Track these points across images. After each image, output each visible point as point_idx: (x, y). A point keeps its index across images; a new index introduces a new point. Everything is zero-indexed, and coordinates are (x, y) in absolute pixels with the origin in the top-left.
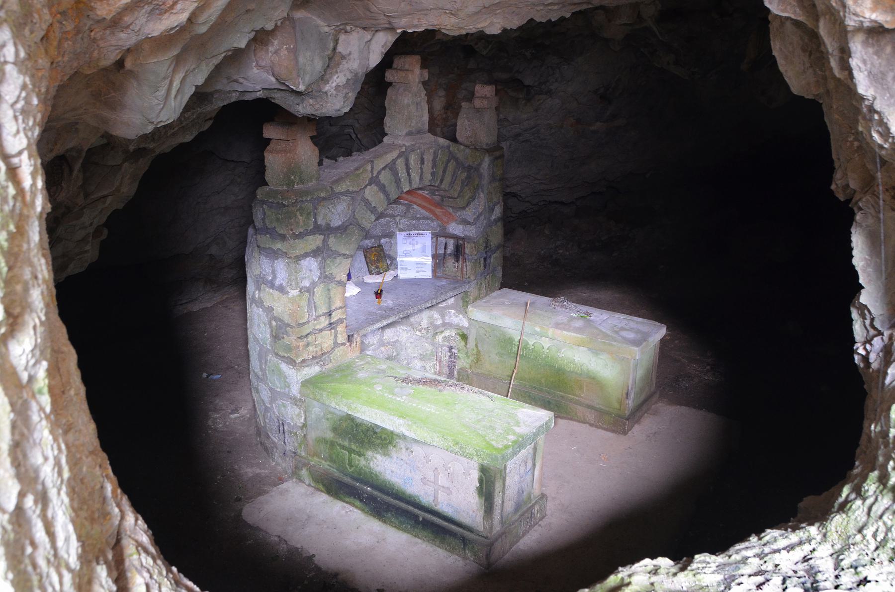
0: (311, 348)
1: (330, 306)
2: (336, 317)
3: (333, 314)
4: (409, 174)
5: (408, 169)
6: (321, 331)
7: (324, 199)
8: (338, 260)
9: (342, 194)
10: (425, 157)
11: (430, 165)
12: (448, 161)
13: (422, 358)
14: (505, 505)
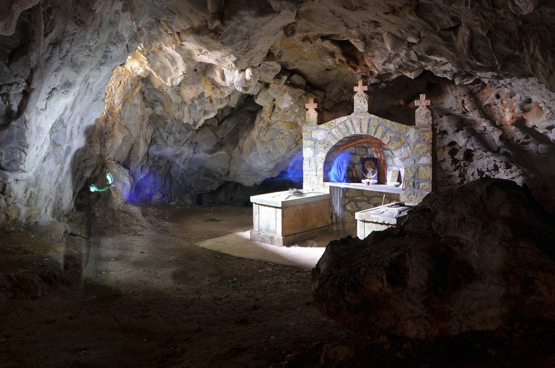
9: (322, 129)
10: (363, 122)
11: (366, 126)
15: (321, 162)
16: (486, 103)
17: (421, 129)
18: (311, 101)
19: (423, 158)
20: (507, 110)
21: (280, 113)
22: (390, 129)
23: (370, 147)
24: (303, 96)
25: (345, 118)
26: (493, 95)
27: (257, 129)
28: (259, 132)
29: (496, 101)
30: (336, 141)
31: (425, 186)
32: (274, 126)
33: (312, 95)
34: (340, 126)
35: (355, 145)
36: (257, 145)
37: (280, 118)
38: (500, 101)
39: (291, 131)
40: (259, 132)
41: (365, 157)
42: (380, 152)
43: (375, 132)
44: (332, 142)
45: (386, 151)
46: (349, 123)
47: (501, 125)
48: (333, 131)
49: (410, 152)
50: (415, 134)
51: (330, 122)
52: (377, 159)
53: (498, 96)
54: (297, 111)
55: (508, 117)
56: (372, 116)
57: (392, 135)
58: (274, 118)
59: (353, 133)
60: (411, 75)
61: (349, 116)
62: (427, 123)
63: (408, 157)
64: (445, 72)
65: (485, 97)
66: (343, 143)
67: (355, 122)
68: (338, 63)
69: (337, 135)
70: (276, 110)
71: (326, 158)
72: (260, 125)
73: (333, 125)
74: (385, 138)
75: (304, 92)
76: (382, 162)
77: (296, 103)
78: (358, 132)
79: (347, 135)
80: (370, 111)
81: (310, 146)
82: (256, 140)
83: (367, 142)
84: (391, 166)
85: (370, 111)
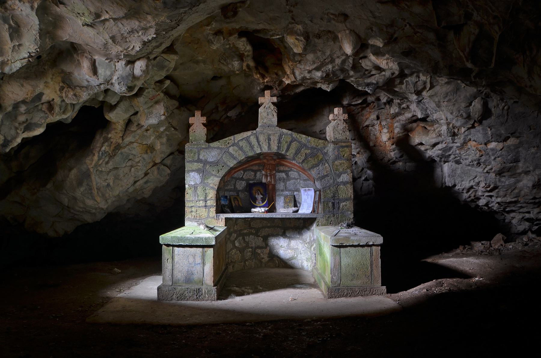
0: (194, 214)
1: (206, 198)
2: (209, 203)
3: (208, 202)
4: (259, 144)
5: (258, 142)
6: (199, 207)
7: (204, 148)
8: (212, 178)
9: (215, 148)
10: (272, 137)
11: (276, 142)
12: (291, 142)
13: (307, 260)
14: (175, 272)
15: (212, 188)
16: (367, 123)
17: (340, 144)
18: (198, 114)
19: (343, 175)
20: (385, 130)
21: (139, 131)
22: (305, 145)
23: (260, 170)
24: (176, 111)
25: (249, 133)
26: (373, 116)
27: (97, 155)
28: (99, 160)
29: (375, 122)
31: (346, 205)
32: (126, 150)
33: (185, 109)
34: (241, 144)
35: (246, 167)
36: (93, 177)
37: (137, 138)
38: (379, 122)
39: (145, 156)
40: (99, 160)
41: (251, 182)
42: (271, 176)
44: (229, 163)
45: (280, 174)
46: (253, 140)
47: (375, 146)
48: (231, 150)
49: (328, 169)
50: (334, 150)
51: (227, 139)
52: (265, 183)
53: (378, 118)
54: (162, 129)
56: (284, 131)
57: (308, 151)
58: (128, 139)
59: (259, 151)
60: (327, 88)
61: (255, 132)
62: (344, 138)
63: (327, 176)
64: (368, 85)
65: (364, 118)
66: (238, 165)
67: (261, 138)
68: (244, 67)
69: (236, 155)
70: (133, 128)
71: (220, 183)
72: (103, 148)
73: (231, 142)
74: (299, 156)
75: (176, 103)
76: (270, 187)
77: (166, 119)
78: (265, 149)
79: (251, 154)
81: (198, 171)
82: (92, 170)
83: (258, 165)
84: (282, 191)
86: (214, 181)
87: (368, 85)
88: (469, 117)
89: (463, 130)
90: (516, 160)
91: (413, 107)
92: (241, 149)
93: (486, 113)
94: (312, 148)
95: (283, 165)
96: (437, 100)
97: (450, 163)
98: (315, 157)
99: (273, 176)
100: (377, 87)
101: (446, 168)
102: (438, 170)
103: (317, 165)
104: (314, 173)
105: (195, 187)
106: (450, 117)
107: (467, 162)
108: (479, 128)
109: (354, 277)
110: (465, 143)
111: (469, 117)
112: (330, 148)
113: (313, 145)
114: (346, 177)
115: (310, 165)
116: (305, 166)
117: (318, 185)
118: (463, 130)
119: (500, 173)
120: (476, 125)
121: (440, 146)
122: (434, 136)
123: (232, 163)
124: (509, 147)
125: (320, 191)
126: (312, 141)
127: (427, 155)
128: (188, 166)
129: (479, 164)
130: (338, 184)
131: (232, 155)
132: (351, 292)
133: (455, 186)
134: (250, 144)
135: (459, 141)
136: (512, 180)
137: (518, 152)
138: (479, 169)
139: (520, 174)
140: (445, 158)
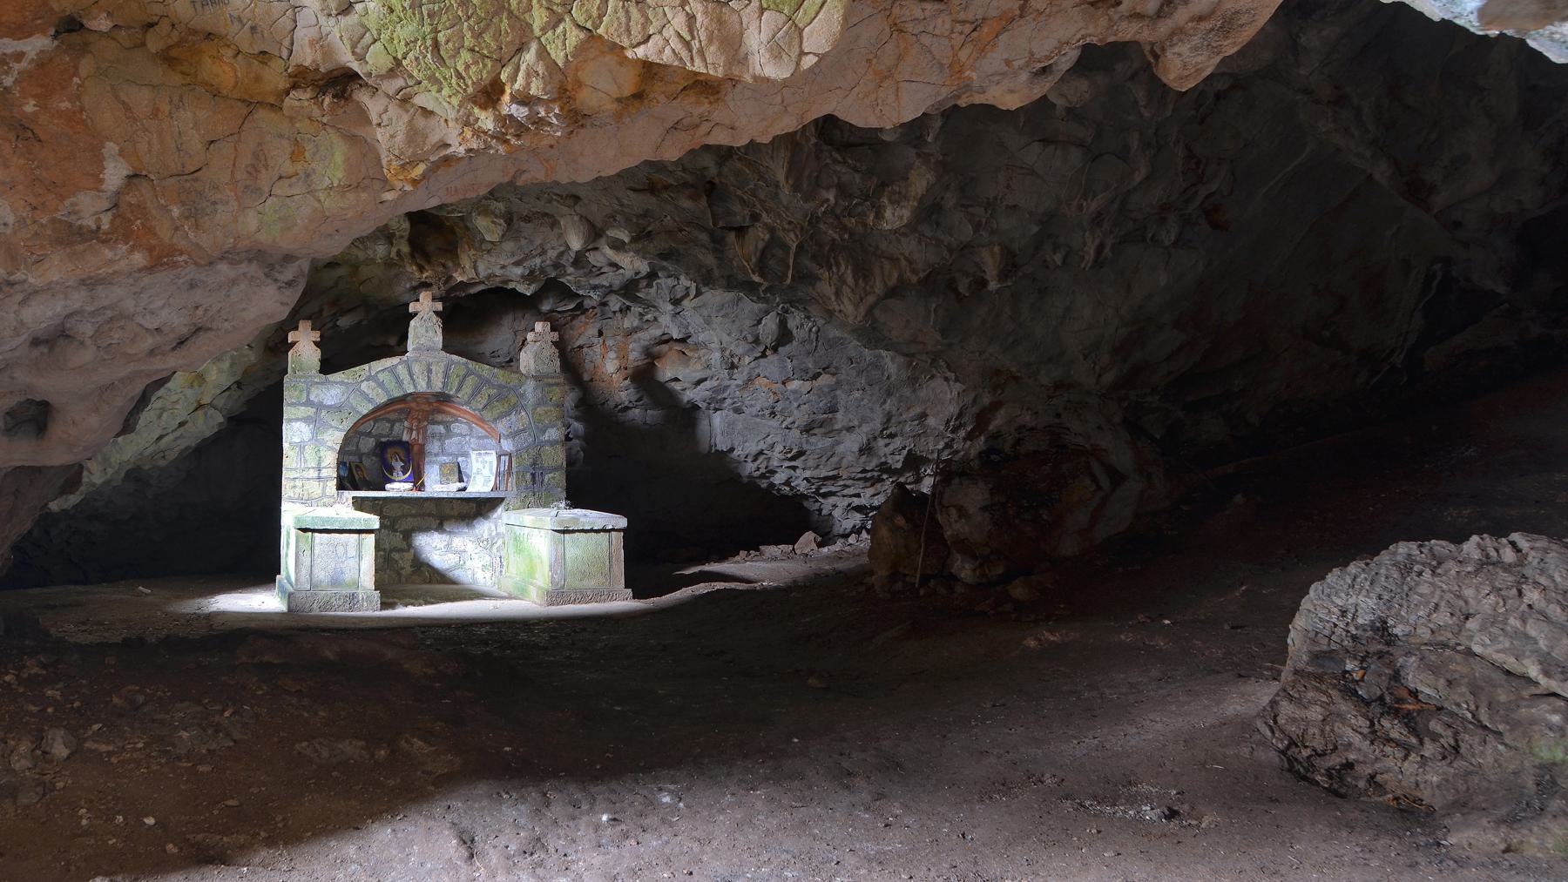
5: (411, 375)
11: (440, 376)
15: (331, 448)
22: (488, 382)
25: (395, 360)
30: (371, 407)
34: (381, 377)
43: (458, 390)
48: (364, 386)
55: (610, 366)
56: (455, 357)
57: (493, 392)
59: (411, 390)
63: (523, 431)
67: (416, 368)
73: (365, 374)
78: (422, 386)
80: (447, 348)
81: (307, 420)
85: (447, 348)
86: (334, 438)
87: (595, 288)
88: (757, 341)
89: (747, 359)
90: (833, 410)
91: (665, 320)
92: (381, 385)
93: (784, 336)
94: (500, 386)
95: (444, 412)
96: (705, 313)
97: (724, 413)
98: (505, 401)
99: (422, 430)
100: (610, 291)
101: (717, 419)
102: (703, 425)
103: (508, 414)
104: (501, 426)
105: (301, 447)
106: (726, 339)
107: (754, 410)
108: (771, 357)
109: (584, 575)
110: (750, 380)
111: (757, 341)
112: (529, 387)
113: (502, 381)
114: (554, 434)
115: (496, 413)
116: (488, 415)
117: (507, 445)
118: (747, 359)
119: (808, 429)
120: (768, 352)
121: (707, 384)
122: (699, 367)
123: (365, 409)
124: (820, 389)
125: (510, 455)
126: (500, 376)
127: (686, 399)
128: (288, 412)
129: (773, 414)
130: (542, 444)
131: (365, 396)
132: (583, 597)
133: (732, 449)
134: (397, 377)
135: (740, 377)
136: (828, 441)
137: (835, 397)
138: (774, 423)
139: (840, 431)
140: (716, 403)
